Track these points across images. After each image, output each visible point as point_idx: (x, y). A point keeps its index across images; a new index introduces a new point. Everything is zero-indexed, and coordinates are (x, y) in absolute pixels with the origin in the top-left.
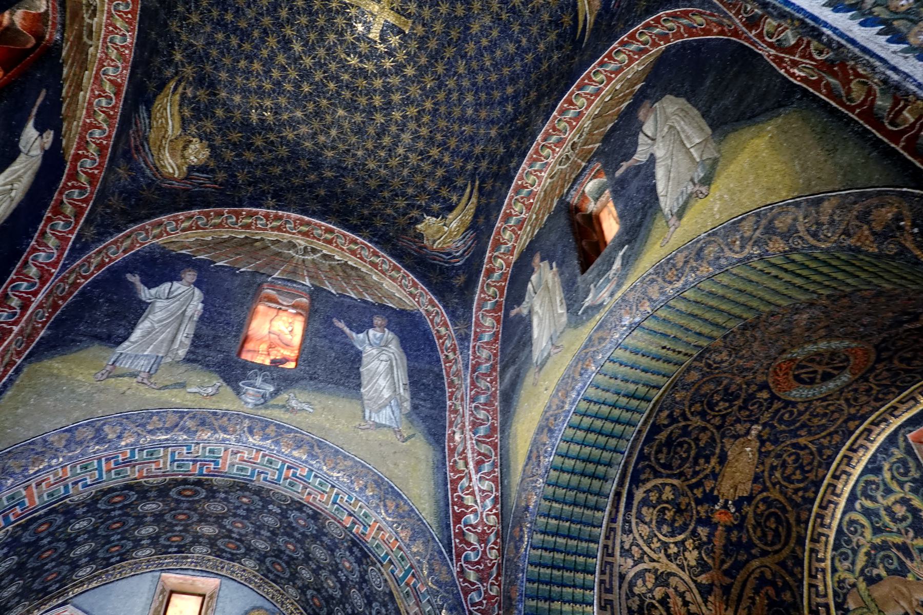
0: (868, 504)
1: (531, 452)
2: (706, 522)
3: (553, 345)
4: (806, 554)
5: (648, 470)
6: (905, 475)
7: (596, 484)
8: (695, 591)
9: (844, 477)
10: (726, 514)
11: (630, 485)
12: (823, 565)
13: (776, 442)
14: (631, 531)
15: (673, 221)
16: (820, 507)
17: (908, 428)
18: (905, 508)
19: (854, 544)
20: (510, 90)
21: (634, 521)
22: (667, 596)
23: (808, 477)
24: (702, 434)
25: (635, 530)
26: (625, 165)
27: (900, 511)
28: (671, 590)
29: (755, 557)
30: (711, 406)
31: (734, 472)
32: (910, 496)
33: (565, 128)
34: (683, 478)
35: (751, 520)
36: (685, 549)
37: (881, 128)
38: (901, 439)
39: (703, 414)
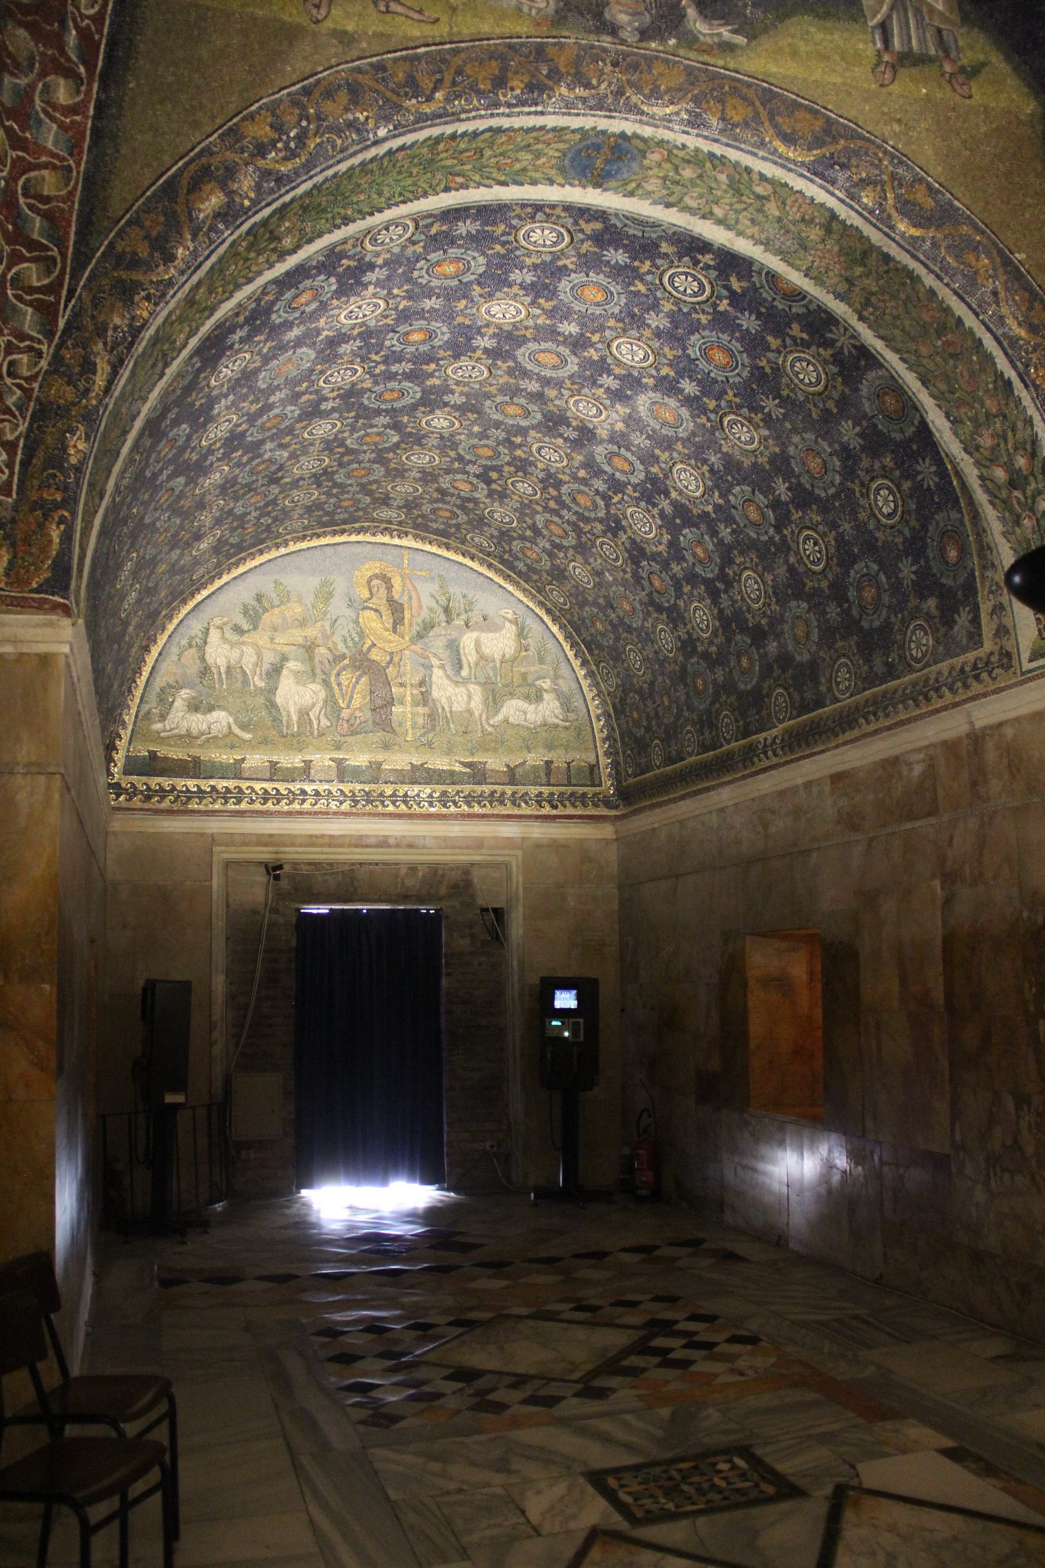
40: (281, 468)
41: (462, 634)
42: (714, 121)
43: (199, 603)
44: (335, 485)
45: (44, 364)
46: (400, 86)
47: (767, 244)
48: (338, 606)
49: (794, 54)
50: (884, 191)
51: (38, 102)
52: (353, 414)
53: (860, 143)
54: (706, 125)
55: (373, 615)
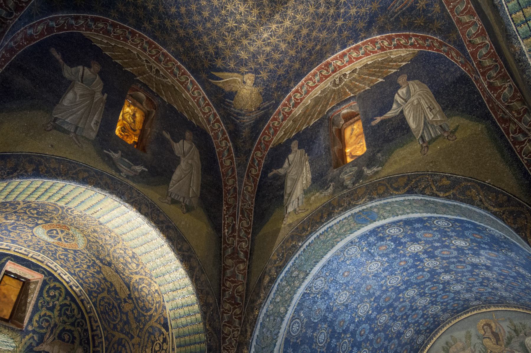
1: (9, 157)
3: (75, 132)
15: (169, 199)
17: (13, 259)
20: (183, 10)
26: (168, 136)
30: (35, 209)
33: (167, 65)
37: (224, 276)
38: (5, 259)
40: (412, 307)
41: (525, 339)
42: (376, 197)
43: (429, 350)
44: (442, 303)
45: (239, 333)
46: (301, 231)
47: (427, 212)
48: (474, 340)
49: (396, 162)
50: (431, 187)
51: (236, 271)
52: (415, 286)
53: (420, 177)
54: (374, 199)
55: (488, 340)
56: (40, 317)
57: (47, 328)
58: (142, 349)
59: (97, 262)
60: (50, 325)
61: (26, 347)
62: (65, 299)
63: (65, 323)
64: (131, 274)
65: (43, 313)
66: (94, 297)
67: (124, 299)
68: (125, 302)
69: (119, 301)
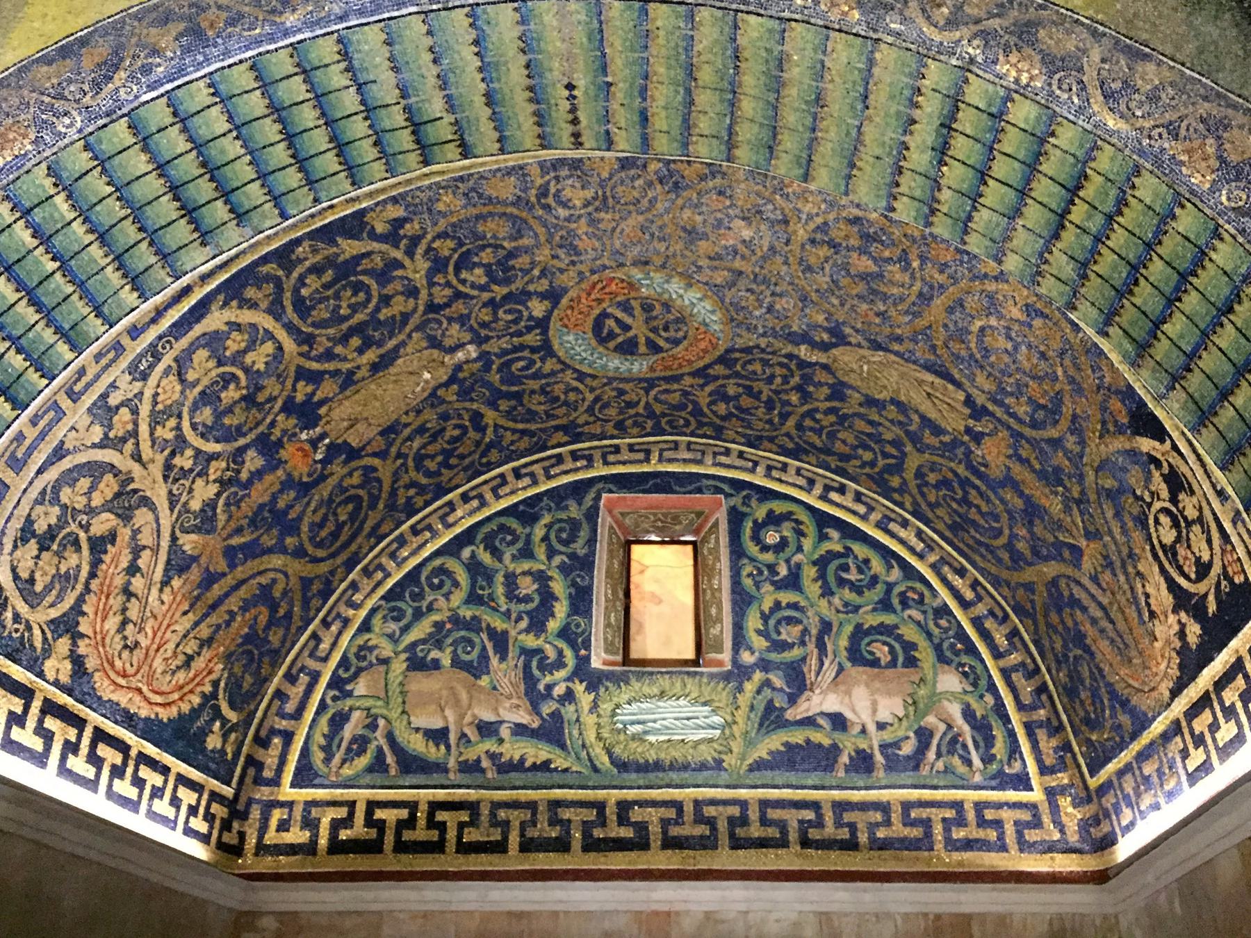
0: (486, 558)
2: (269, 447)
4: (343, 586)
5: (270, 288)
6: (566, 543)
7: (182, 231)
8: (163, 557)
9: (475, 503)
10: (306, 455)
11: (218, 290)
12: (351, 612)
13: (464, 394)
14: (144, 377)
16: (412, 527)
18: (536, 586)
19: (424, 604)
21: (167, 360)
22: (112, 537)
23: (440, 474)
24: (400, 298)
25: (152, 381)
27: (527, 586)
28: (125, 534)
29: (283, 550)
30: (464, 262)
31: (376, 398)
32: (554, 573)
34: (306, 348)
35: (325, 490)
36: (203, 474)
38: (591, 495)
39: (439, 265)
56: (765, 618)
57: (803, 643)
58: (1126, 574)
59: (803, 351)
60: (805, 631)
61: (756, 717)
62: (823, 537)
63: (857, 609)
64: (916, 315)
65: (767, 605)
66: (902, 489)
67: (968, 431)
68: (978, 438)
69: (960, 452)
